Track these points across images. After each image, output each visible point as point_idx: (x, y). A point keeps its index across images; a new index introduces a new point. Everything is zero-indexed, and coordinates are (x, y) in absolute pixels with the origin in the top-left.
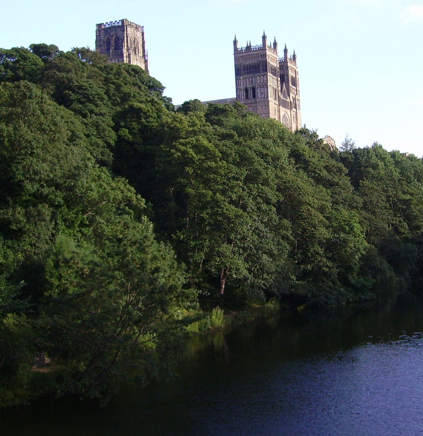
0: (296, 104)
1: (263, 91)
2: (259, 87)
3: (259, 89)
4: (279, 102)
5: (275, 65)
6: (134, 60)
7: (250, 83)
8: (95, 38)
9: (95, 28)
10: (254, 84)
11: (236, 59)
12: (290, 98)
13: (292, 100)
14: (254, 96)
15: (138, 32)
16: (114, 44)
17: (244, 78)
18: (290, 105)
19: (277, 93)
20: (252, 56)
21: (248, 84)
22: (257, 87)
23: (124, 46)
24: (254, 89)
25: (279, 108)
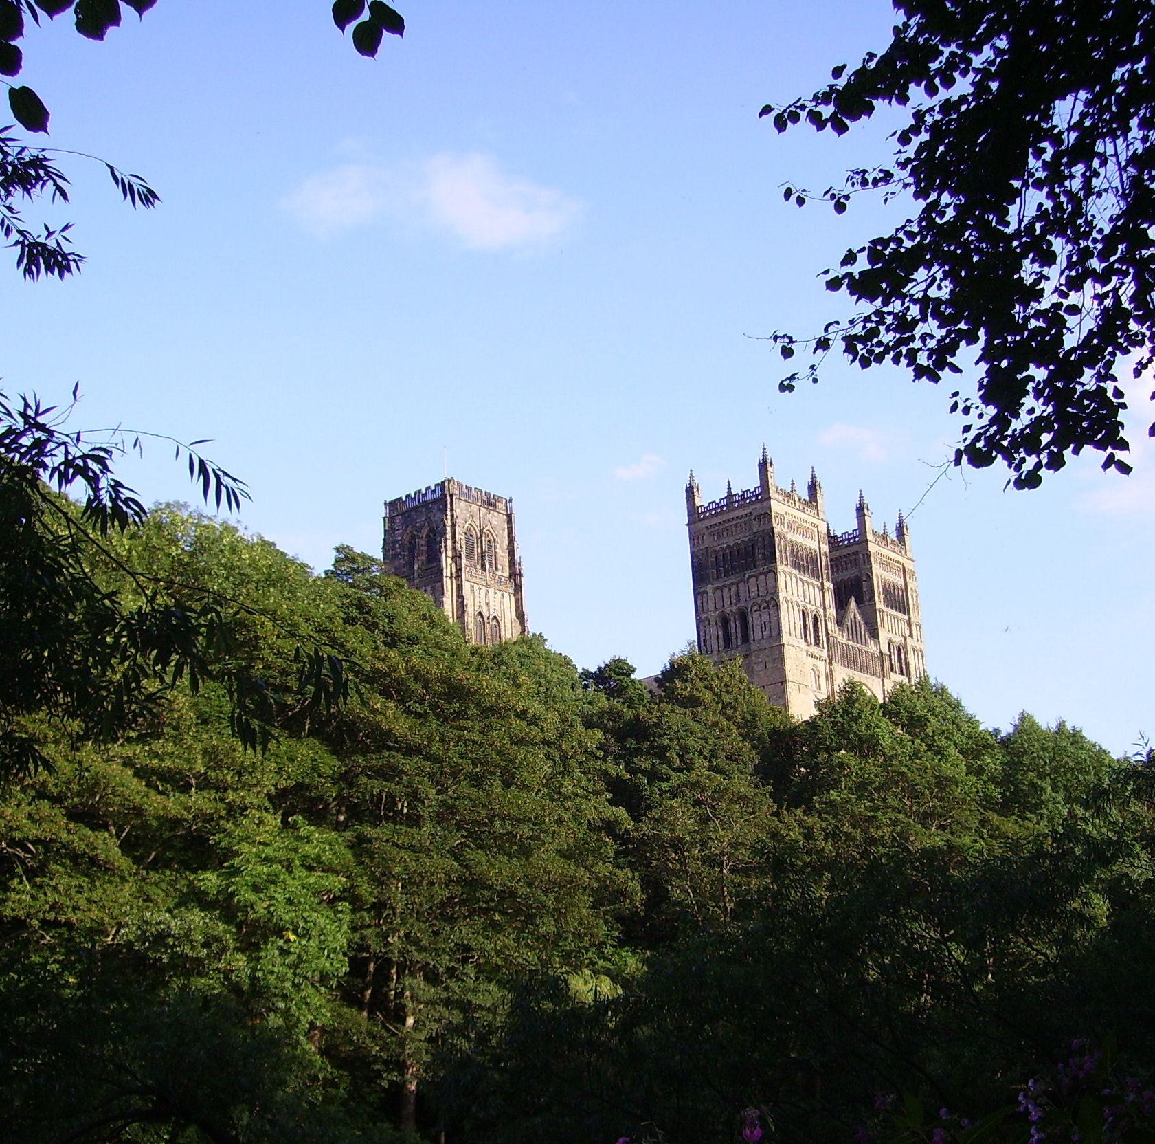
0: (907, 664)
1: (765, 618)
2: (755, 608)
3: (756, 615)
4: (828, 651)
5: (814, 545)
6: (476, 587)
7: (734, 601)
8: (383, 536)
9: (383, 512)
10: (742, 604)
11: (693, 537)
12: (878, 644)
13: (885, 650)
14: (746, 638)
15: (496, 513)
16: (425, 548)
17: (717, 588)
18: (878, 662)
19: (821, 625)
20: (734, 522)
21: (729, 603)
22: (749, 609)
23: (443, 550)
24: (743, 616)
25: (831, 670)
